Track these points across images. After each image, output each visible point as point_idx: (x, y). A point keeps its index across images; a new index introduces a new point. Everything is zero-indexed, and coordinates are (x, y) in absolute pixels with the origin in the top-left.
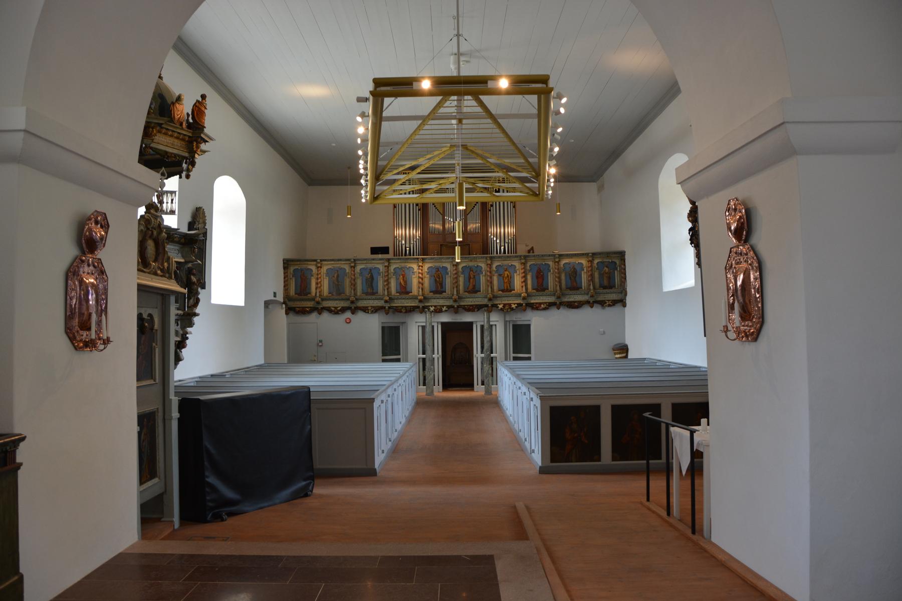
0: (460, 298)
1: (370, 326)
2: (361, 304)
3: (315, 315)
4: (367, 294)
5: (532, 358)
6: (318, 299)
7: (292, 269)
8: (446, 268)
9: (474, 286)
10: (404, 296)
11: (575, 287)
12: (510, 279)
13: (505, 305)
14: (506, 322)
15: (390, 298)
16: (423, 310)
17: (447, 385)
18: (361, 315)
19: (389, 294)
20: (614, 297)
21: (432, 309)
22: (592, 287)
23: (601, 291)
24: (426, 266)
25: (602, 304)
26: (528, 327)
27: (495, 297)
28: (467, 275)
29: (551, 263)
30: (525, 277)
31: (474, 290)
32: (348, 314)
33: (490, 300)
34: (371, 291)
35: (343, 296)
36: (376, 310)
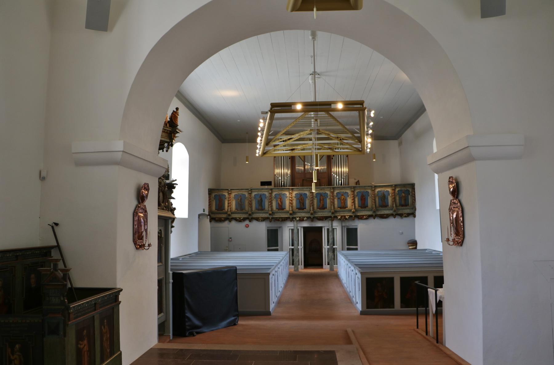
0: (315, 212)
1: (260, 229)
2: (255, 216)
3: (227, 222)
4: (258, 210)
5: (359, 249)
6: (229, 213)
7: (213, 195)
8: (306, 194)
9: (323, 205)
10: (281, 211)
11: (384, 205)
12: (345, 201)
13: (342, 217)
14: (342, 227)
15: (273, 213)
16: (292, 219)
17: (307, 265)
18: (255, 223)
19: (272, 210)
20: (408, 211)
21: (298, 219)
22: (394, 206)
23: (400, 208)
24: (294, 193)
25: (401, 215)
26: (356, 229)
27: (336, 212)
29: (369, 191)
30: (354, 199)
31: (323, 207)
32: (247, 222)
33: (333, 213)
34: (261, 207)
35: (244, 211)
36: (264, 219)
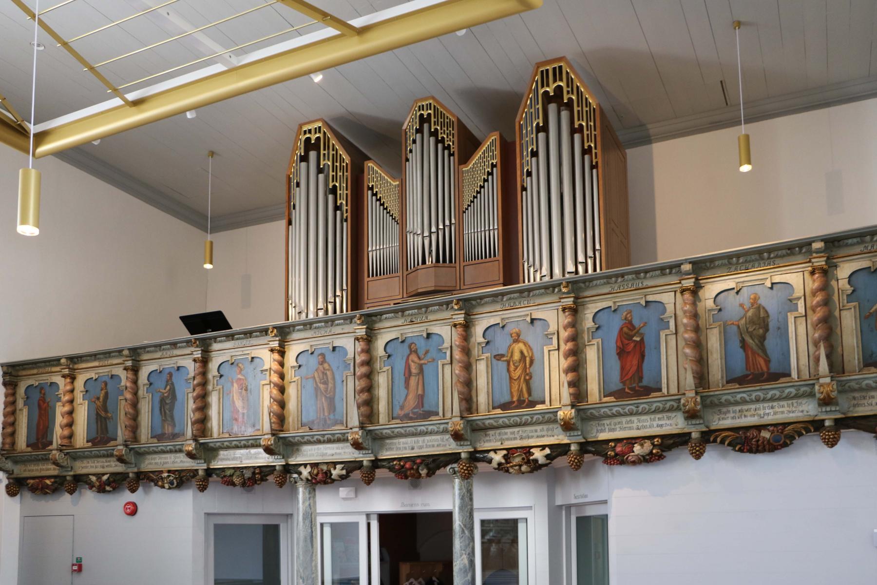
9: (421, 398)
28: (400, 366)
29: (667, 298)
30: (576, 354)
